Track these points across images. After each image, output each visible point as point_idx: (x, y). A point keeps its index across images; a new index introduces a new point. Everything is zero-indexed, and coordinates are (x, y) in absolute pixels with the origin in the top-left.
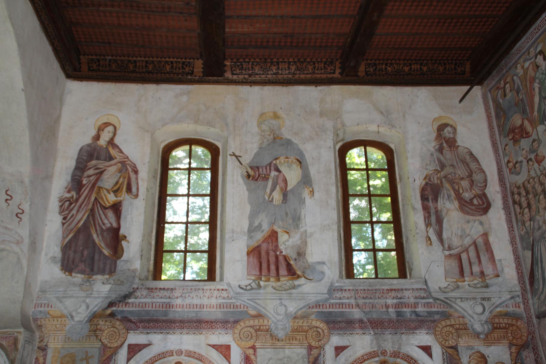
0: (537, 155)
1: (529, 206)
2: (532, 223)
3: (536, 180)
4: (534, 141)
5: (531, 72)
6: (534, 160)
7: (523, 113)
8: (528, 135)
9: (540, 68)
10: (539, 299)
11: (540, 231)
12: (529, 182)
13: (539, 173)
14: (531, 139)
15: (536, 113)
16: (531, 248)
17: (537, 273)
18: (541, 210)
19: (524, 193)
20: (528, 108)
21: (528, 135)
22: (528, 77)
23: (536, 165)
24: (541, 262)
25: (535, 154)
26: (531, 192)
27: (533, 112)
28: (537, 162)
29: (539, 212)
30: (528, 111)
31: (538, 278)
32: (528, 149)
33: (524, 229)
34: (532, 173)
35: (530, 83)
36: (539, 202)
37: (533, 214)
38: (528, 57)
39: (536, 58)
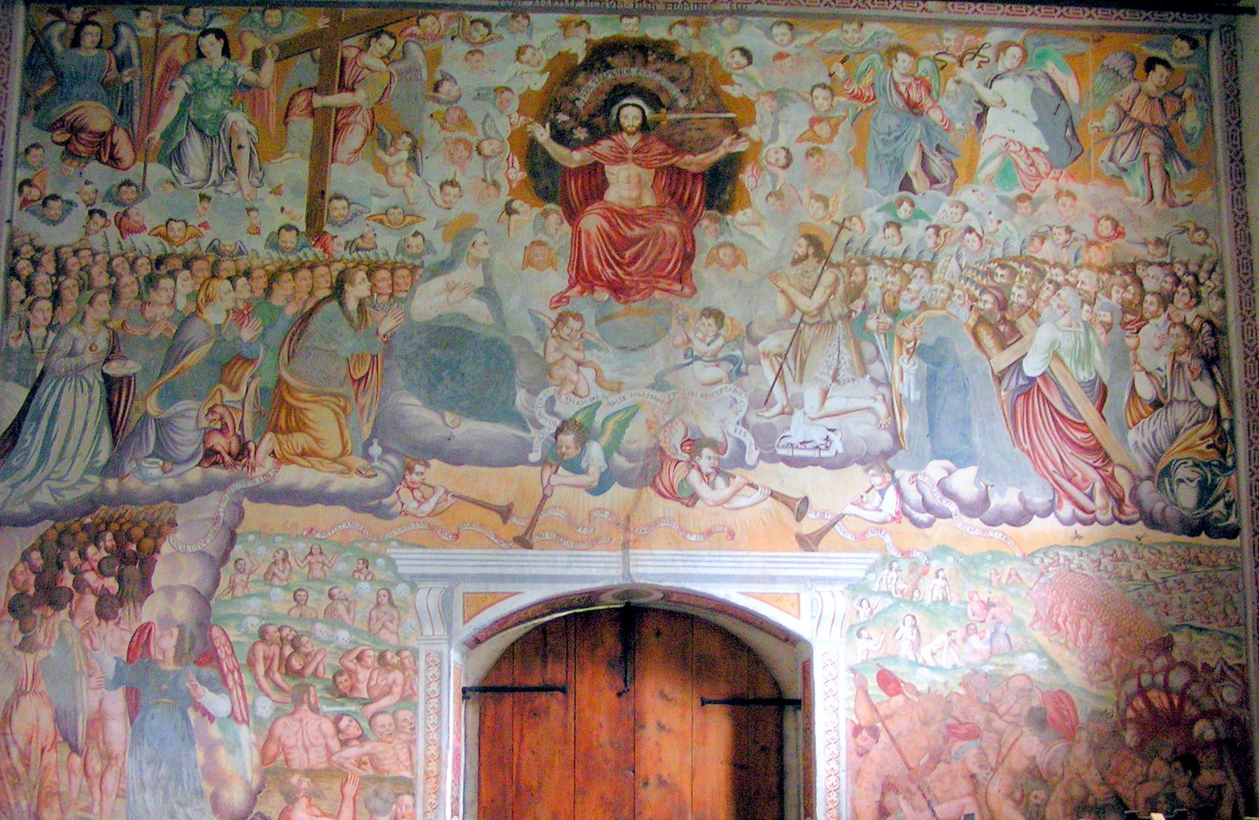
0: (125, 214)
1: (56, 298)
2: (52, 335)
3: (98, 258)
4: (128, 183)
5: (178, 51)
6: (111, 217)
7: (121, 113)
8: (114, 161)
9: (204, 62)
10: (13, 486)
11: (74, 361)
12: (76, 252)
13: (114, 249)
14: (120, 176)
15: (156, 134)
16: (31, 383)
17: (29, 437)
18: (89, 319)
19: (51, 267)
20: (137, 112)
21: (114, 161)
22: (166, 55)
23: (113, 231)
24: (53, 419)
25: (122, 210)
26: (73, 274)
27: (150, 123)
28: (119, 227)
29: (82, 321)
30: (136, 118)
31: (27, 449)
32: (103, 189)
33: (24, 339)
34: (97, 241)
35: (167, 69)
36: (91, 302)
37: (62, 319)
38: (180, 17)
39: (205, 33)
